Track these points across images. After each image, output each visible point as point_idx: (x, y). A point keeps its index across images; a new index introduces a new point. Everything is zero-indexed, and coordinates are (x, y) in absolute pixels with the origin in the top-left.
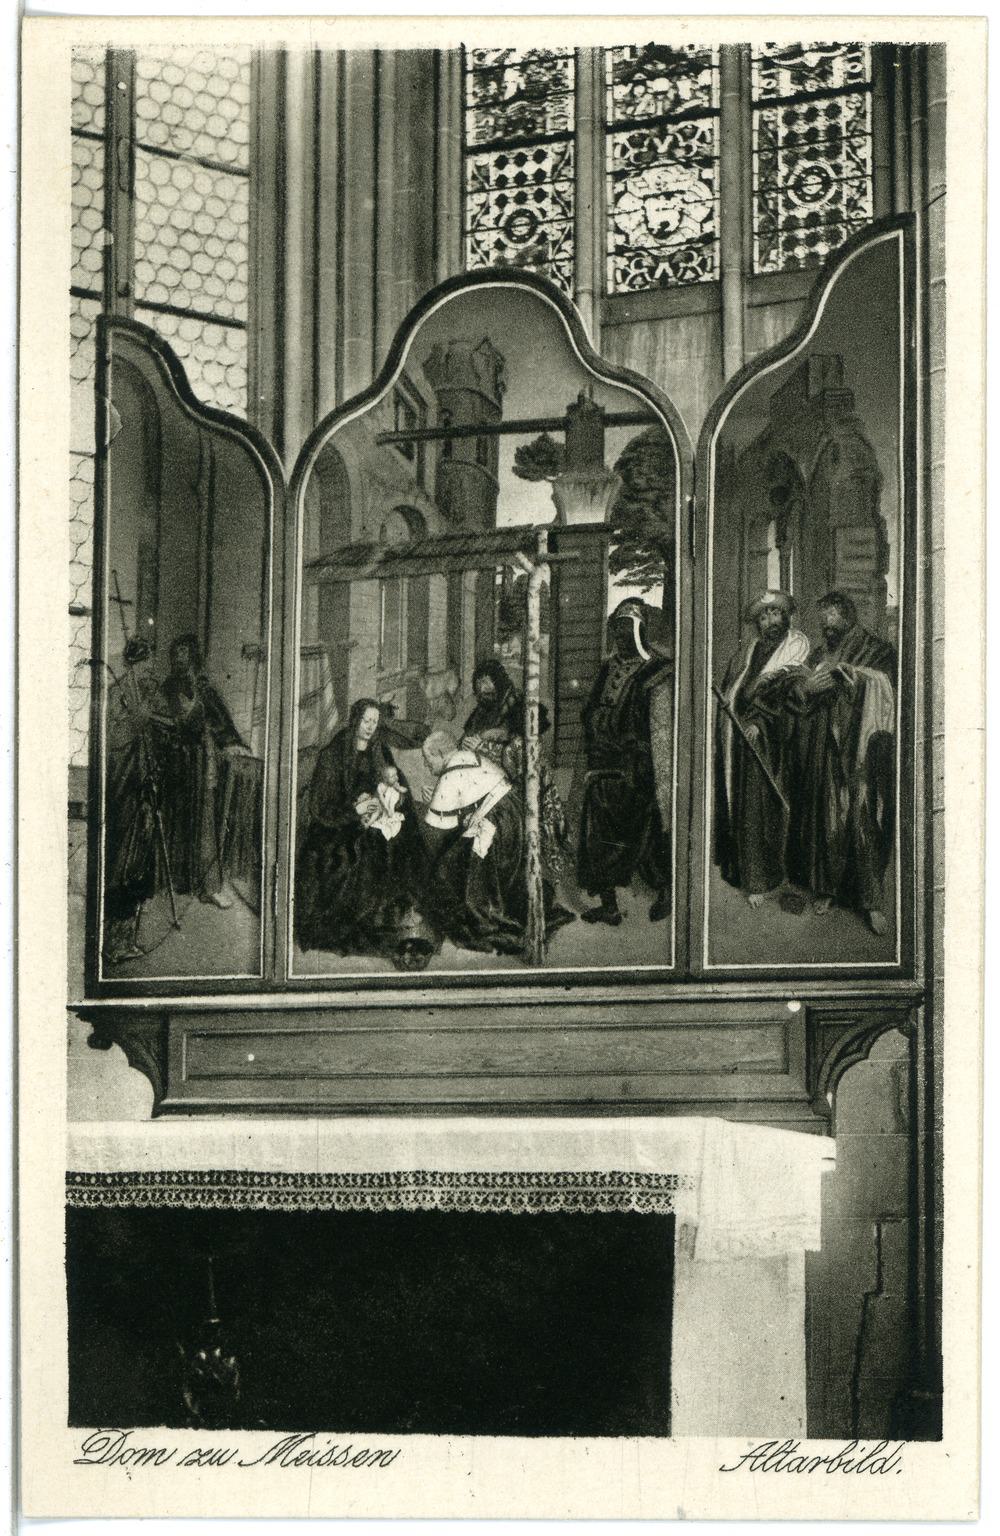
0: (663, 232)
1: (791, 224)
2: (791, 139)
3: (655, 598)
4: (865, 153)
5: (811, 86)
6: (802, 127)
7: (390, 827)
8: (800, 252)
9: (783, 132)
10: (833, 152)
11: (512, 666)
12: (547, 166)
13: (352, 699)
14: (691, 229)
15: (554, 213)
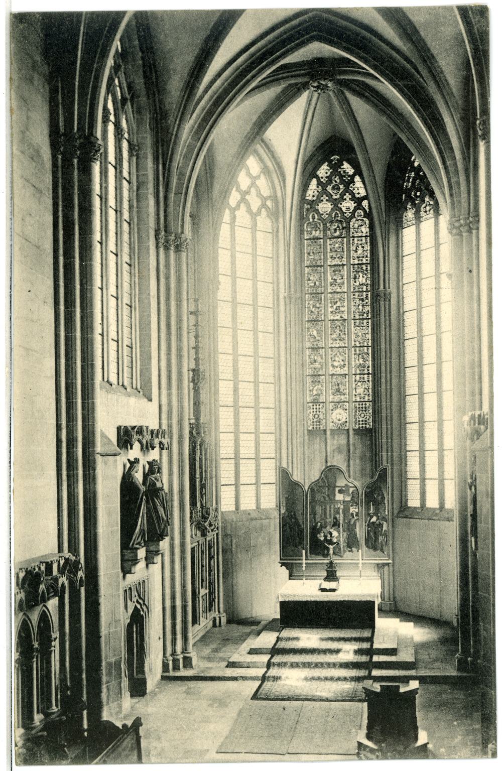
0: (339, 420)
1: (359, 421)
2: (359, 408)
3: (357, 510)
4: (371, 411)
5: (362, 400)
6: (361, 406)
7: (322, 539)
8: (361, 426)
9: (358, 406)
10: (366, 411)
11: (338, 518)
12: (320, 407)
13: (317, 521)
14: (344, 420)
15: (322, 415)
